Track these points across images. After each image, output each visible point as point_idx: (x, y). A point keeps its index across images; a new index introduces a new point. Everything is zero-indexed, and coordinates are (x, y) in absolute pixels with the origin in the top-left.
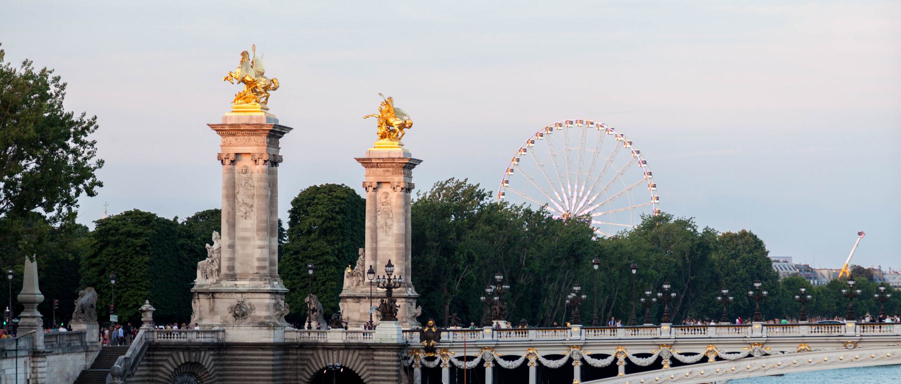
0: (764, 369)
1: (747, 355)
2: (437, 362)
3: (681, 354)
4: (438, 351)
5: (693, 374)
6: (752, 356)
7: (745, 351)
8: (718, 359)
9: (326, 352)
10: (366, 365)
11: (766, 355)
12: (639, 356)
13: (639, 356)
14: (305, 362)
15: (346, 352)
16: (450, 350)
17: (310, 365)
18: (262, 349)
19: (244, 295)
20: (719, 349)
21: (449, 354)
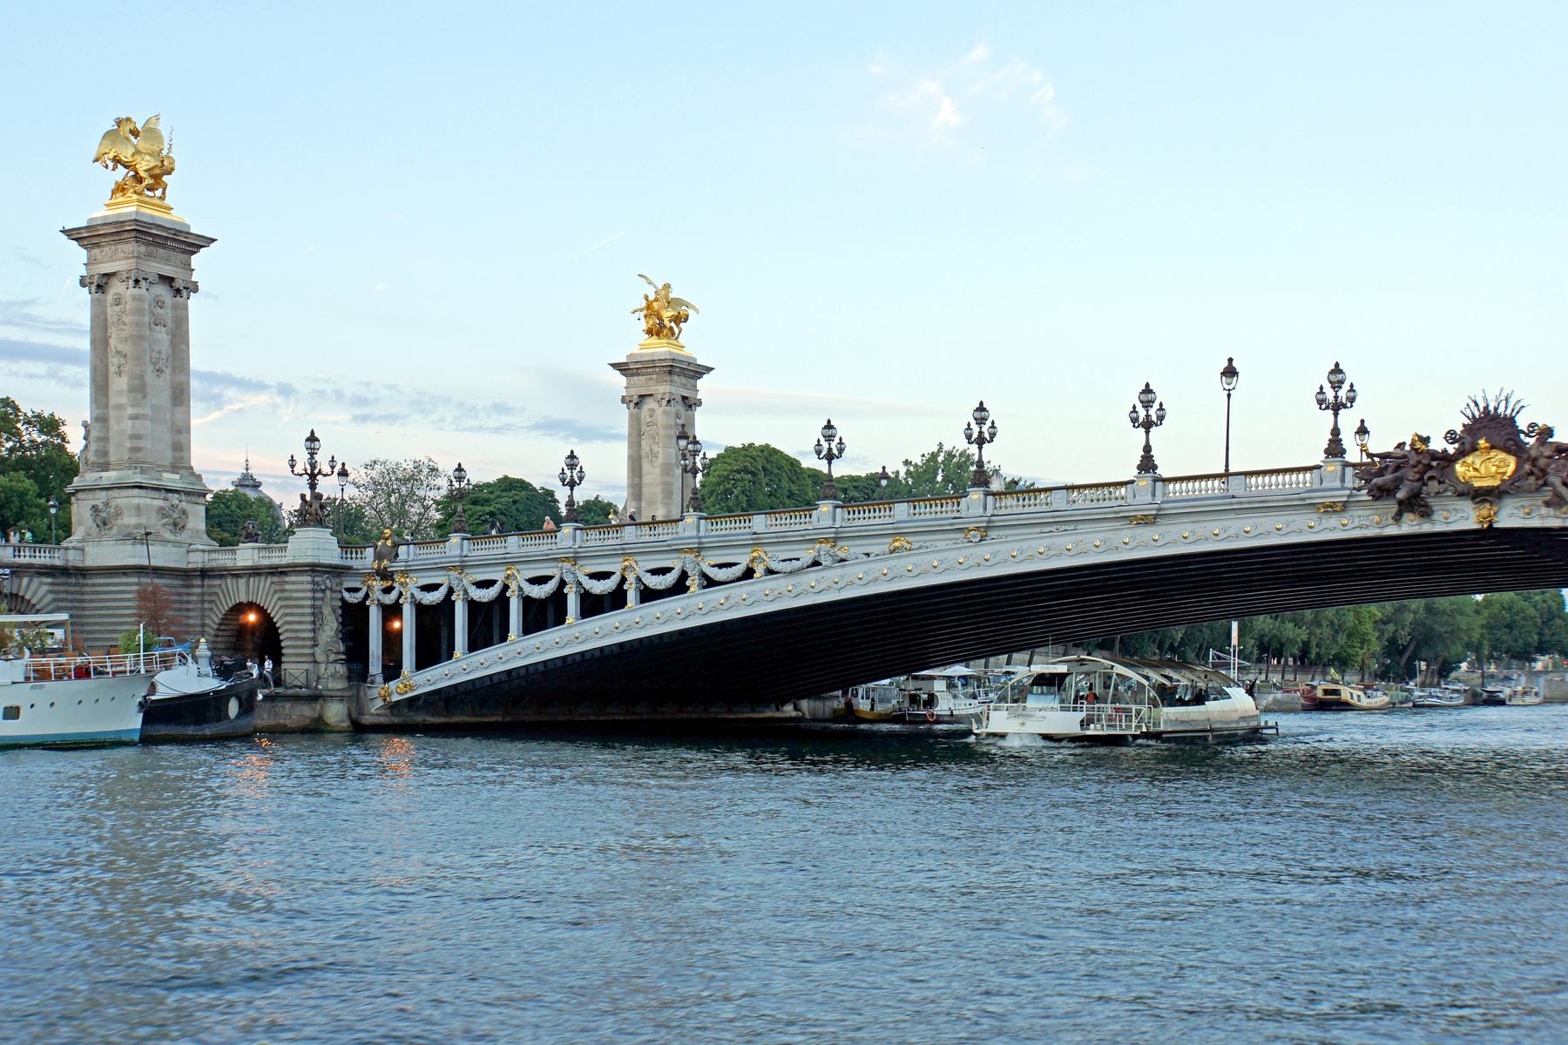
0: (838, 586)
1: (810, 562)
2: (394, 595)
3: (714, 566)
4: (396, 577)
5: (732, 601)
6: (821, 564)
7: (807, 555)
8: (770, 572)
9: (235, 581)
10: (279, 599)
11: (842, 560)
12: (655, 572)
13: (655, 572)
14: (213, 598)
15: (257, 579)
16: (411, 575)
17: (218, 602)
18: (124, 574)
19: (110, 493)
20: (770, 555)
21: (408, 580)
